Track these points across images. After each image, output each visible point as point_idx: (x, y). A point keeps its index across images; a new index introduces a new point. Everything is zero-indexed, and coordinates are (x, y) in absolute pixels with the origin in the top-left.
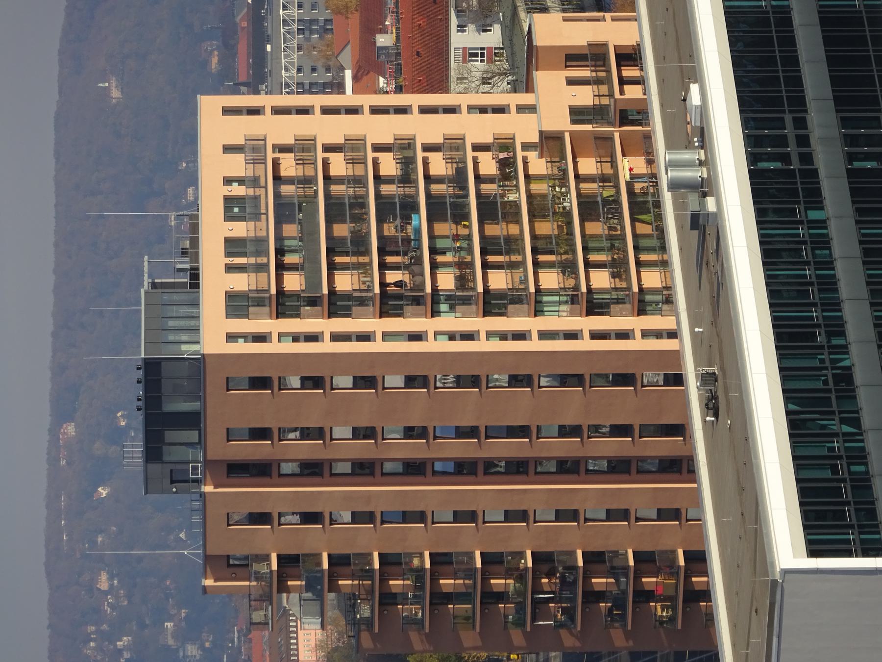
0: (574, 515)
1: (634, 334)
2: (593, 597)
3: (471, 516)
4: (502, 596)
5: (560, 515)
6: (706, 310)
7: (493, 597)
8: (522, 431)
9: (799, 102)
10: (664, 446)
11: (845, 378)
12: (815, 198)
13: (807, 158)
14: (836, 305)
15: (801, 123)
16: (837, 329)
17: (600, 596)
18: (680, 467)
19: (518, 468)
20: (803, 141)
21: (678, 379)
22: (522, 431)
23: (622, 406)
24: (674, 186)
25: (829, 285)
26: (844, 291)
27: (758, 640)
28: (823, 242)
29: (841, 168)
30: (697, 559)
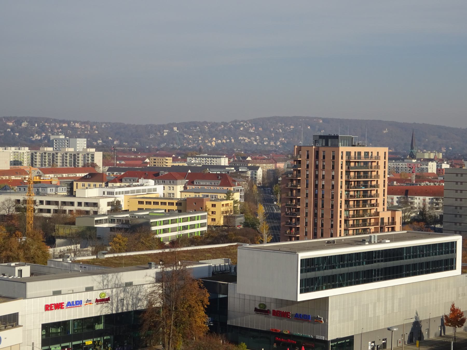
0: (306, 216)
1: (341, 228)
2: (291, 219)
3: (307, 196)
4: (292, 202)
5: (307, 213)
6: (347, 242)
7: (291, 200)
8: (323, 207)
9: (386, 261)
10: (319, 233)
11: (334, 267)
12: (368, 263)
13: (375, 262)
14: (347, 266)
15: (382, 261)
16: (343, 266)
17: (291, 220)
18: (315, 236)
19: (316, 206)
20: (378, 261)
21: (332, 236)
22: (323, 207)
23: (327, 226)
24: (371, 237)
25: (351, 265)
26: (350, 268)
27: (285, 249)
28: (359, 264)
29: (373, 268)
30: (297, 239)
